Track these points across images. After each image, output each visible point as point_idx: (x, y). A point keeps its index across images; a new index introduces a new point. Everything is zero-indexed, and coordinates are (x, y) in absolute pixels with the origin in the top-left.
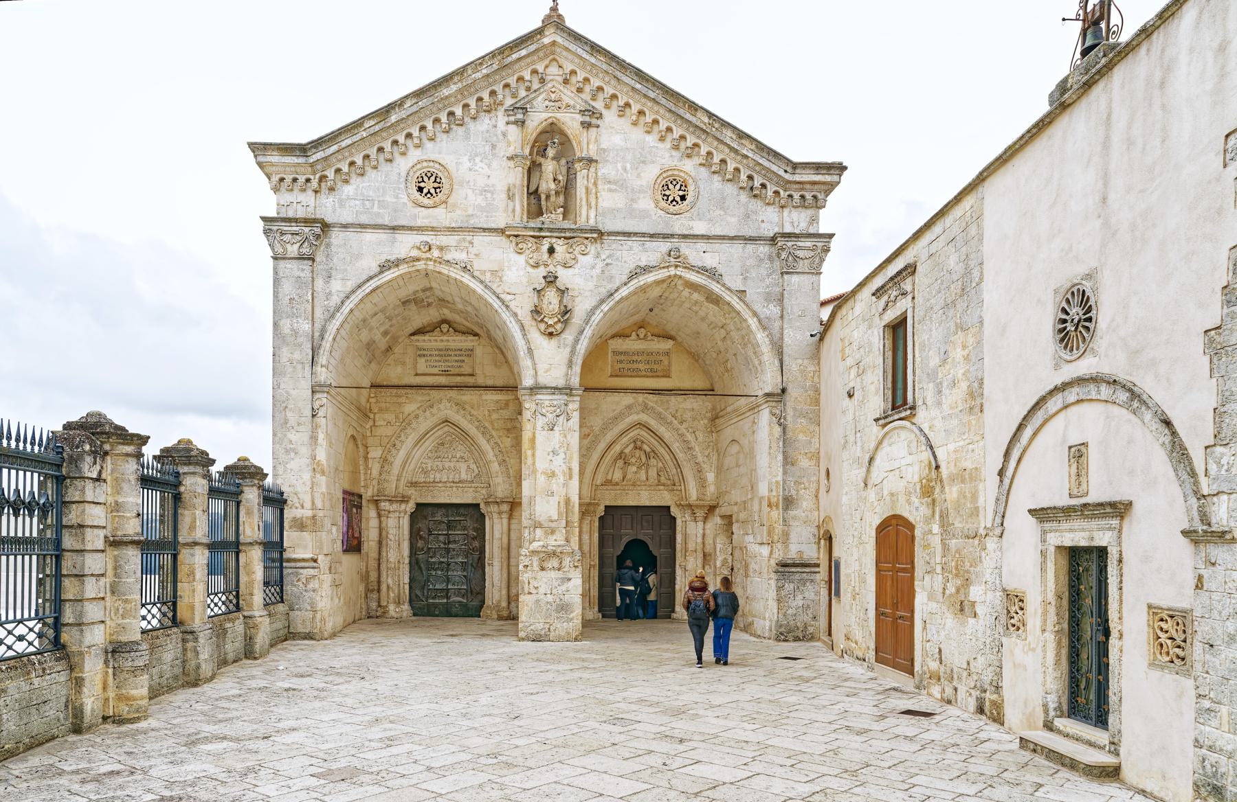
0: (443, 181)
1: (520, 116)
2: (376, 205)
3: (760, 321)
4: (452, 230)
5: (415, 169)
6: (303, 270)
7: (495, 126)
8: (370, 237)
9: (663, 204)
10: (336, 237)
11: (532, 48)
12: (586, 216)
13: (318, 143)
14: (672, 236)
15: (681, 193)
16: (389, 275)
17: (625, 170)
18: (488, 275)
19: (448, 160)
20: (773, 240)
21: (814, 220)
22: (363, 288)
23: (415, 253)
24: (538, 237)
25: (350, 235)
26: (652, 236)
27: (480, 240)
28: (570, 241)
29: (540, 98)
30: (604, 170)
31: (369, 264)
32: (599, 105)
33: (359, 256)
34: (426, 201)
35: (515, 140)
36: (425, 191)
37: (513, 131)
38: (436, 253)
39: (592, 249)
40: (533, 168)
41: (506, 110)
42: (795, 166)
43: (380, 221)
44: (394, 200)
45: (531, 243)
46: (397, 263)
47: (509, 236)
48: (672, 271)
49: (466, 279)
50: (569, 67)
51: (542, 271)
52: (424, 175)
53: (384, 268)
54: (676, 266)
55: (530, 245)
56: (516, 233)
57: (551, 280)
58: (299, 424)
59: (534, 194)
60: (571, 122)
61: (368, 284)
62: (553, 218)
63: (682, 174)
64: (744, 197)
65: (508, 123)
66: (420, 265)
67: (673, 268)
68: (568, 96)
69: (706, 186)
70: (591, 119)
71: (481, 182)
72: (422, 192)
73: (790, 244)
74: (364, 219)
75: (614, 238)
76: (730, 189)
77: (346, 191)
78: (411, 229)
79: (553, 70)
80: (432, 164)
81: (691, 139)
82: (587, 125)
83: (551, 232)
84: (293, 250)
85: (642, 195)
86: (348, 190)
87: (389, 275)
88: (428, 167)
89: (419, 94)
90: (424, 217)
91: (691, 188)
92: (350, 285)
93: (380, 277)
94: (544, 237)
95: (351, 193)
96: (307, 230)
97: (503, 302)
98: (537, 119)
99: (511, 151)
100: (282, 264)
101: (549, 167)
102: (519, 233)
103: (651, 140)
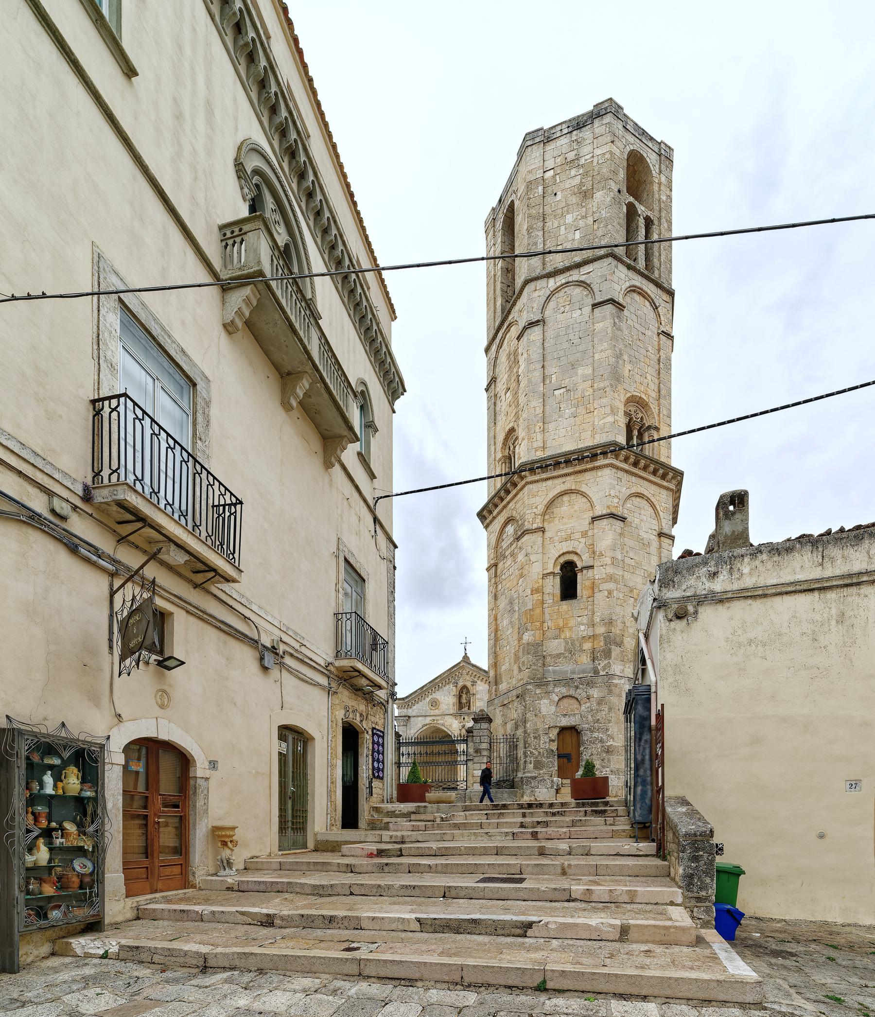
8: (420, 718)
10: (412, 719)
13: (407, 697)
16: (424, 728)
19: (438, 697)
25: (415, 718)
27: (446, 717)
30: (478, 696)
31: (420, 726)
32: (476, 679)
33: (417, 724)
35: (454, 691)
37: (454, 688)
40: (460, 697)
45: (459, 717)
46: (426, 725)
49: (443, 728)
51: (462, 724)
59: (460, 703)
60: (469, 684)
62: (465, 709)
68: (468, 678)
70: (474, 683)
71: (447, 702)
74: (418, 714)
79: (464, 671)
86: (415, 707)
87: (424, 728)
89: (430, 682)
92: (416, 731)
98: (460, 684)
101: (464, 696)
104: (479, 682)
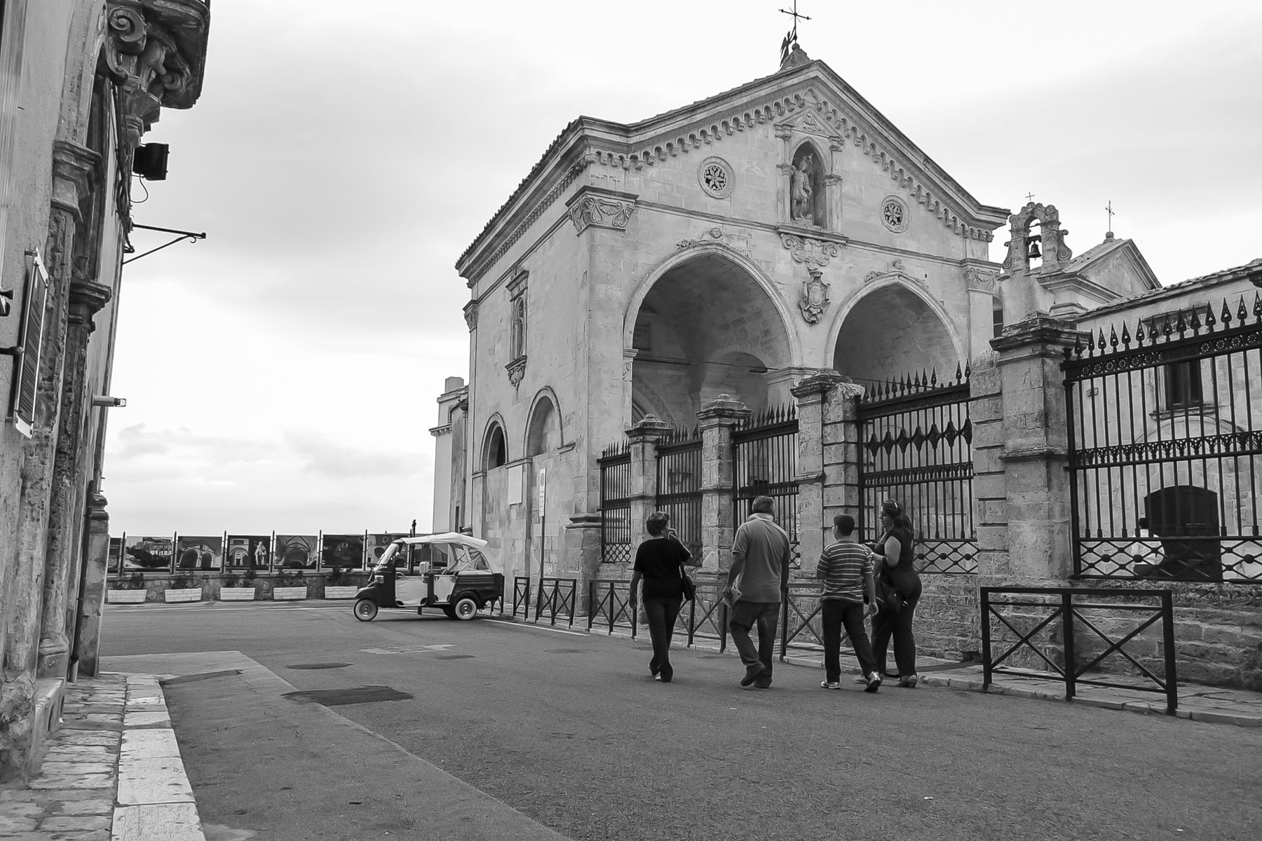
0: (726, 176)
1: (788, 133)
2: (675, 190)
3: (955, 328)
4: (736, 222)
5: (705, 163)
6: (616, 240)
7: (767, 137)
8: (670, 218)
9: (886, 223)
10: (642, 213)
11: (802, 78)
12: (837, 225)
14: (895, 250)
15: (898, 216)
17: (861, 190)
18: (763, 264)
20: (962, 263)
21: (986, 251)
22: (666, 263)
23: (707, 237)
24: (801, 237)
25: (653, 214)
26: (882, 248)
28: (824, 244)
29: (799, 119)
30: (847, 188)
34: (714, 193)
35: (783, 153)
36: (712, 183)
38: (724, 241)
39: (839, 252)
41: (775, 125)
42: (981, 208)
43: (678, 205)
44: (690, 188)
46: (692, 245)
47: (780, 233)
48: (896, 280)
50: (822, 98)
52: (710, 169)
53: (682, 247)
54: (899, 276)
55: (795, 243)
56: (787, 231)
57: (816, 277)
58: (612, 386)
60: (823, 145)
61: (670, 260)
63: (899, 201)
64: (940, 225)
65: (776, 136)
66: (712, 249)
67: (897, 277)
68: (820, 122)
69: (916, 214)
72: (709, 184)
73: (975, 268)
74: (665, 201)
75: (855, 246)
76: (931, 216)
77: (650, 173)
78: (704, 215)
80: (718, 161)
81: (906, 175)
82: (833, 148)
83: (813, 234)
84: (608, 221)
85: (873, 213)
86: (652, 172)
88: (715, 163)
90: (711, 206)
91: (905, 212)
92: (653, 259)
93: (680, 255)
94: (807, 238)
95: (654, 175)
96: (624, 204)
97: (777, 290)
98: (799, 137)
99: (780, 161)
100: (599, 233)
102: (789, 232)
103: (878, 169)
104: (849, 145)
